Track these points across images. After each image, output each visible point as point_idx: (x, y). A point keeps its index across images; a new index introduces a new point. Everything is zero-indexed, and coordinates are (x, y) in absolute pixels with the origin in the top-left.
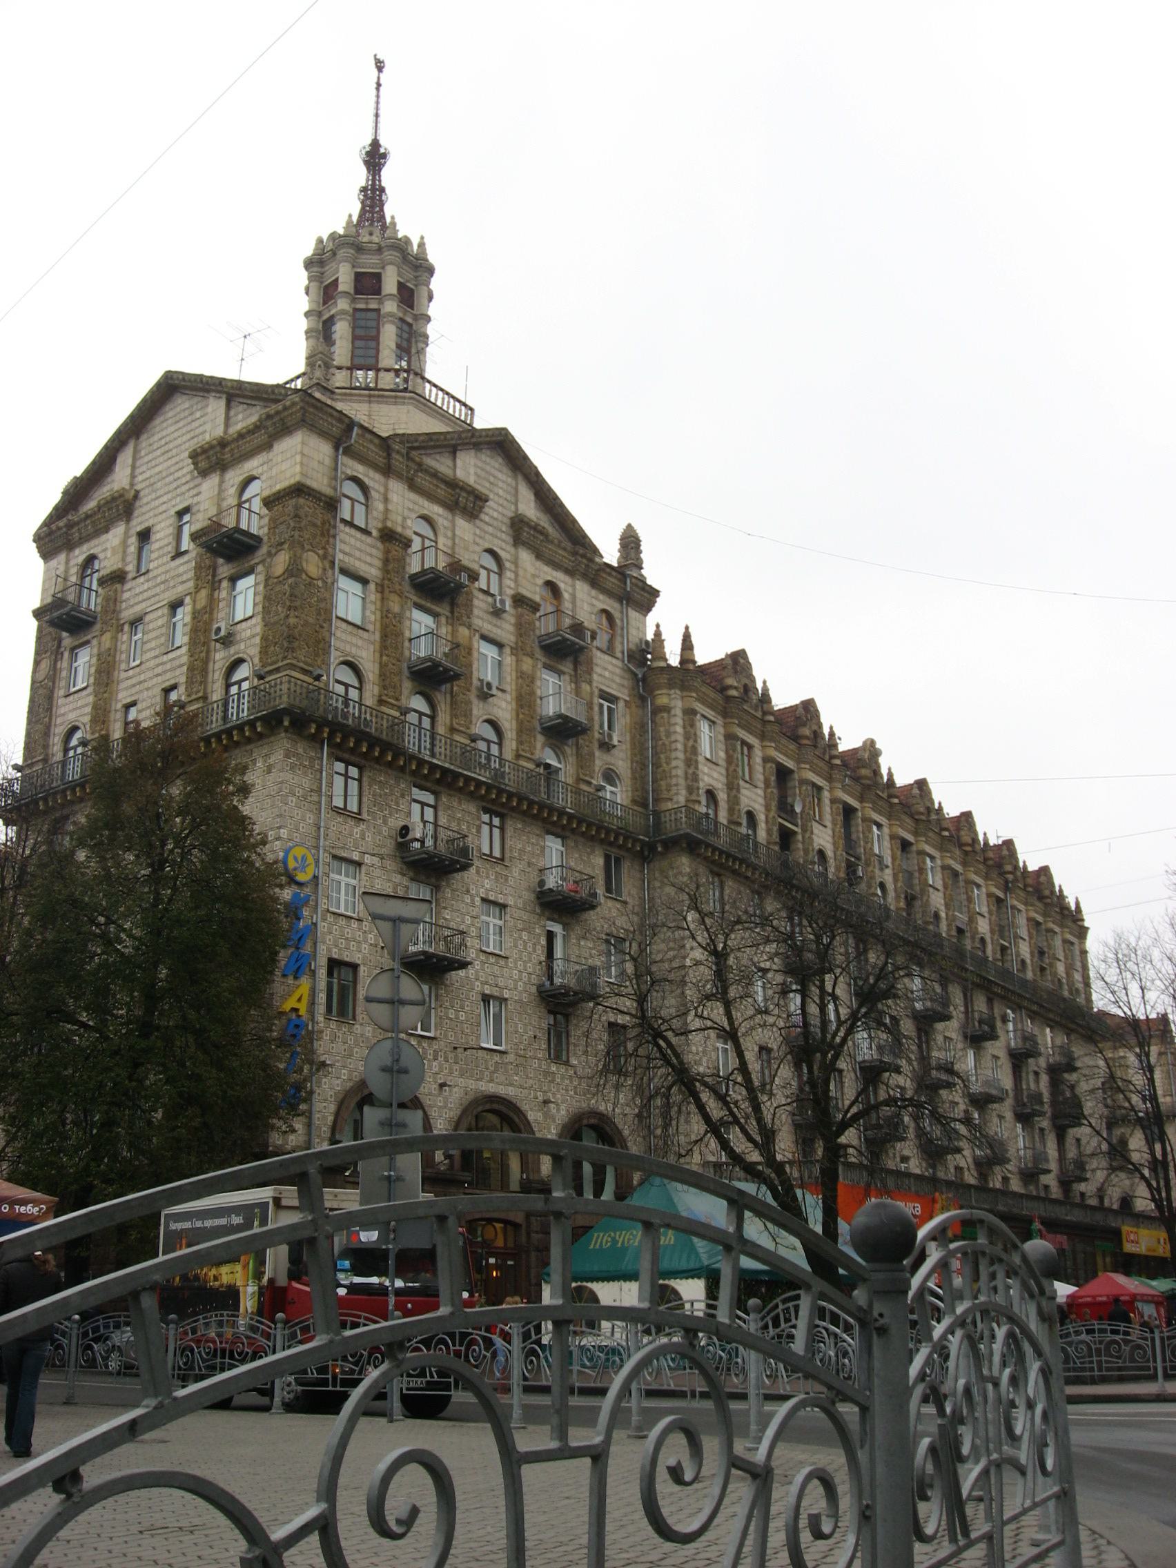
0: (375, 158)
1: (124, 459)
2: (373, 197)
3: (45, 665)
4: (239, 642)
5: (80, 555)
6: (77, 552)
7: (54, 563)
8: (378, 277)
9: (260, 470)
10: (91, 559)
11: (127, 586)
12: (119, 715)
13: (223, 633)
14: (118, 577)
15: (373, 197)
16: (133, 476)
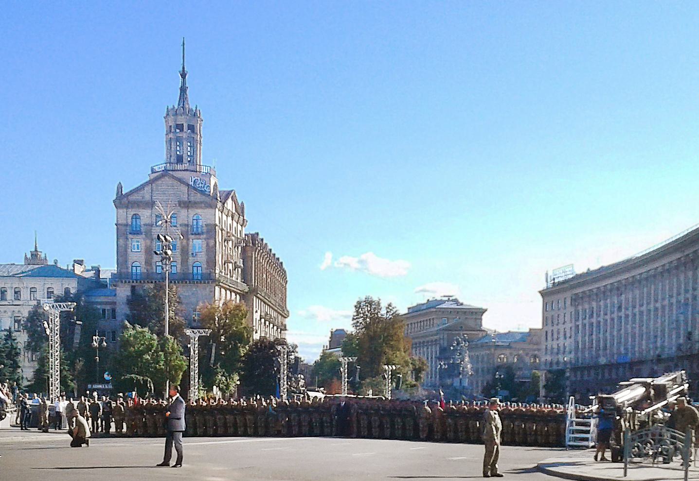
0: (183, 75)
1: (147, 189)
2: (183, 90)
3: (121, 241)
4: (198, 257)
5: (132, 212)
6: (130, 210)
7: (121, 211)
8: (193, 126)
9: (201, 214)
10: (135, 214)
11: (153, 228)
12: (155, 263)
13: (194, 255)
14: (152, 225)
15: (183, 90)
16: (152, 196)
